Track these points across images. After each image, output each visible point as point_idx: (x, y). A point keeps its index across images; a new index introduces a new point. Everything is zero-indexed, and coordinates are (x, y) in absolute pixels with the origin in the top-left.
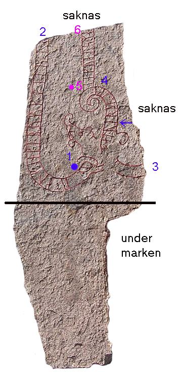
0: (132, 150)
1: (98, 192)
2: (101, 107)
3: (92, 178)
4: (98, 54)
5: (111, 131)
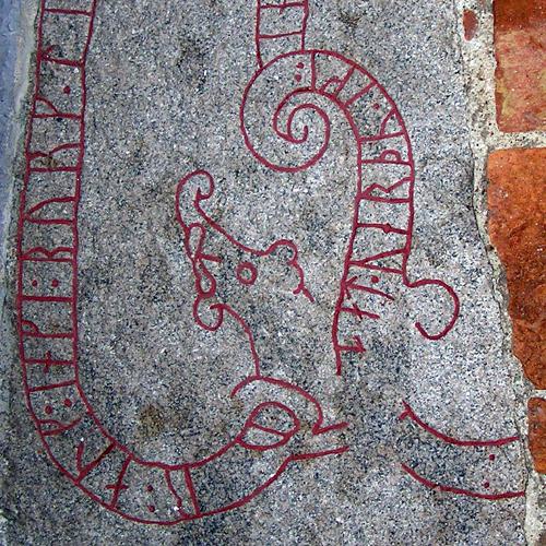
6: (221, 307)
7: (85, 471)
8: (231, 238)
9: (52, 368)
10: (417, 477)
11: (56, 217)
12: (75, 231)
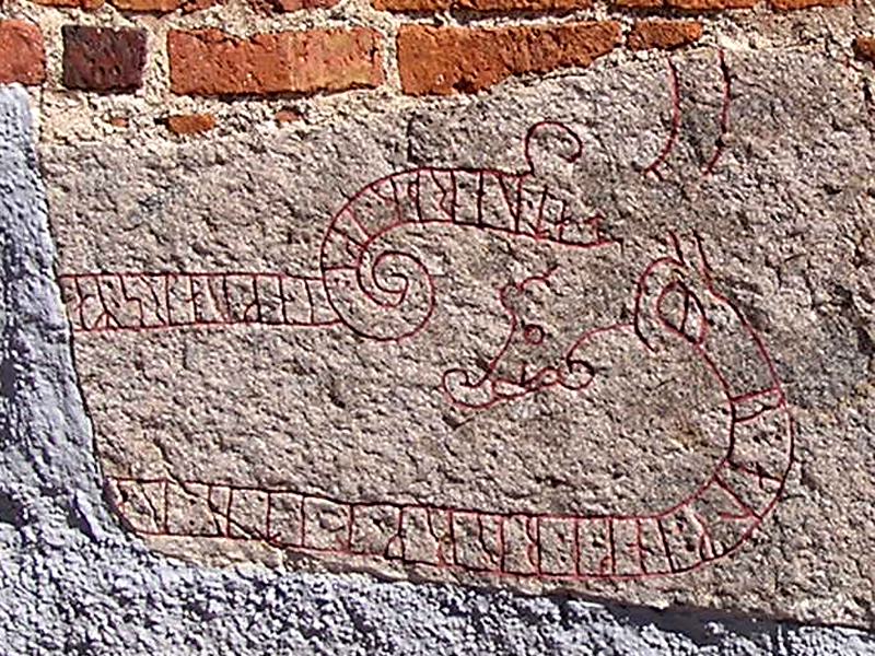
0: (604, 105)
1: (796, 257)
2: (412, 244)
3: (730, 282)
4: (174, 258)
5: (519, 200)
10: (716, 159)
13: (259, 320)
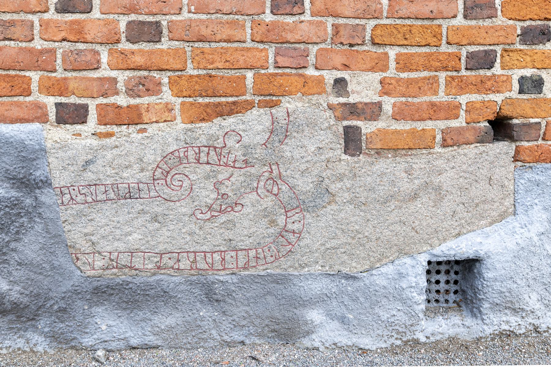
6: (236, 204)
7: (290, 243)
8: (214, 203)
9: (258, 256)
10: (284, 140)
11: (211, 259)
12: (215, 252)
13: (130, 198)
